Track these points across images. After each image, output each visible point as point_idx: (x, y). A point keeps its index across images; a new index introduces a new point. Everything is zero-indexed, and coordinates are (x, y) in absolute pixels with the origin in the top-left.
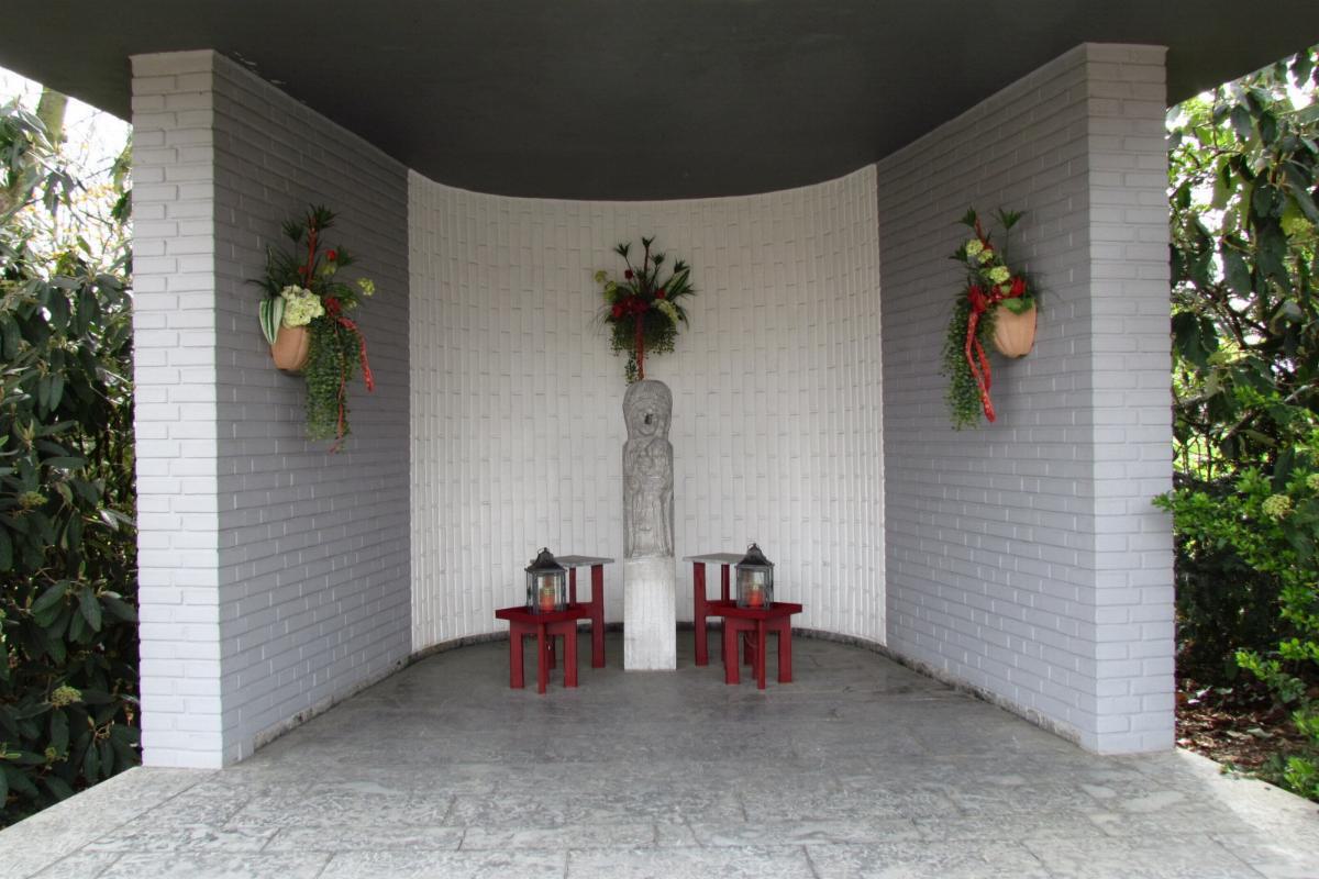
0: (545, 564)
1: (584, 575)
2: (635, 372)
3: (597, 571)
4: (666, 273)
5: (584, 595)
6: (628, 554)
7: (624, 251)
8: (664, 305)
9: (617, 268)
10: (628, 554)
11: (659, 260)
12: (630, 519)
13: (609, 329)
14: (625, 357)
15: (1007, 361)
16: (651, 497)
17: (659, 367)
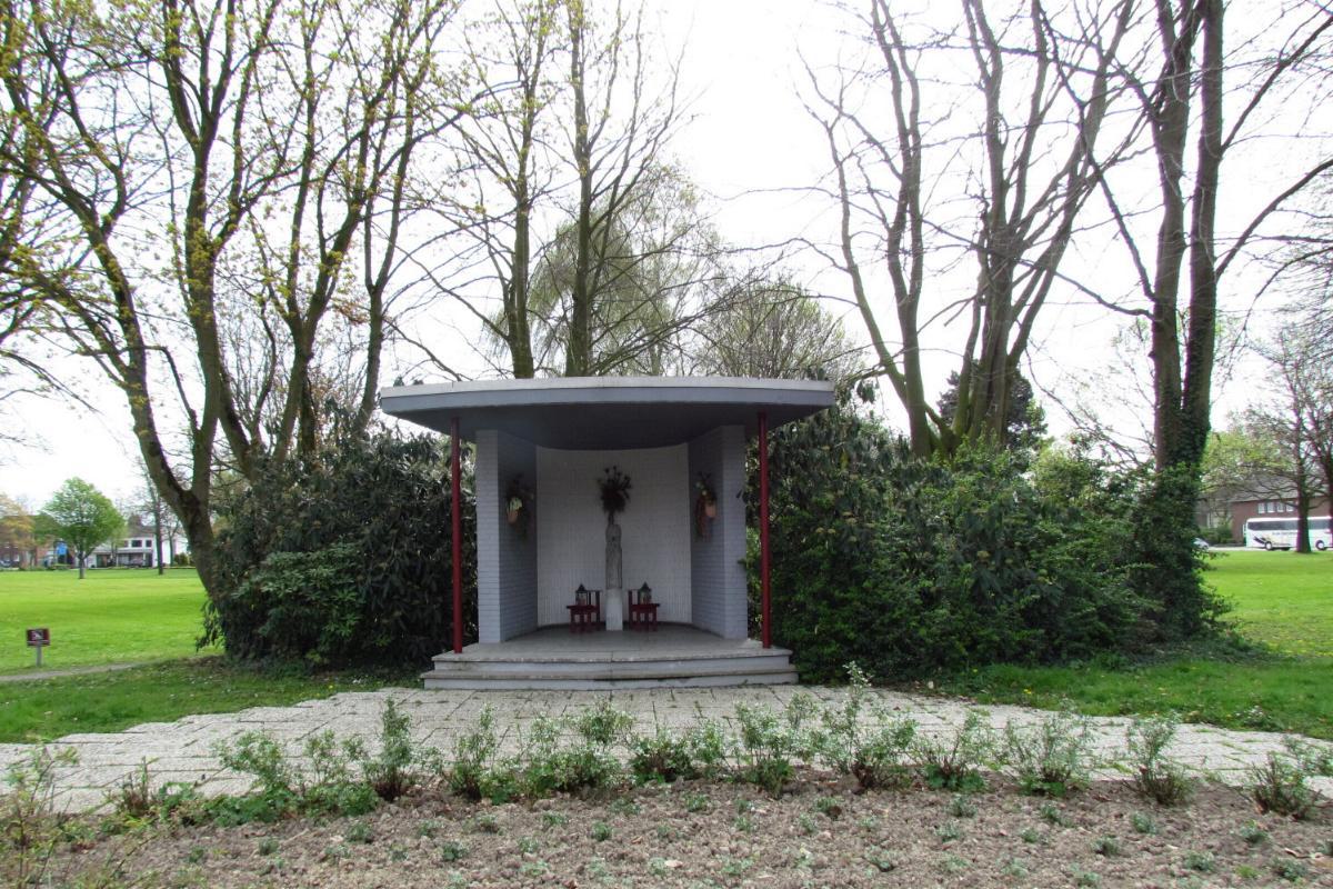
0: (581, 589)
1: (593, 595)
2: (611, 520)
3: (598, 594)
4: (622, 479)
5: (593, 603)
6: (607, 588)
7: (607, 471)
8: (621, 493)
9: (605, 477)
10: (607, 588)
11: (619, 474)
12: (609, 576)
13: (602, 502)
14: (607, 514)
15: (712, 520)
16: (615, 568)
17: (620, 519)
